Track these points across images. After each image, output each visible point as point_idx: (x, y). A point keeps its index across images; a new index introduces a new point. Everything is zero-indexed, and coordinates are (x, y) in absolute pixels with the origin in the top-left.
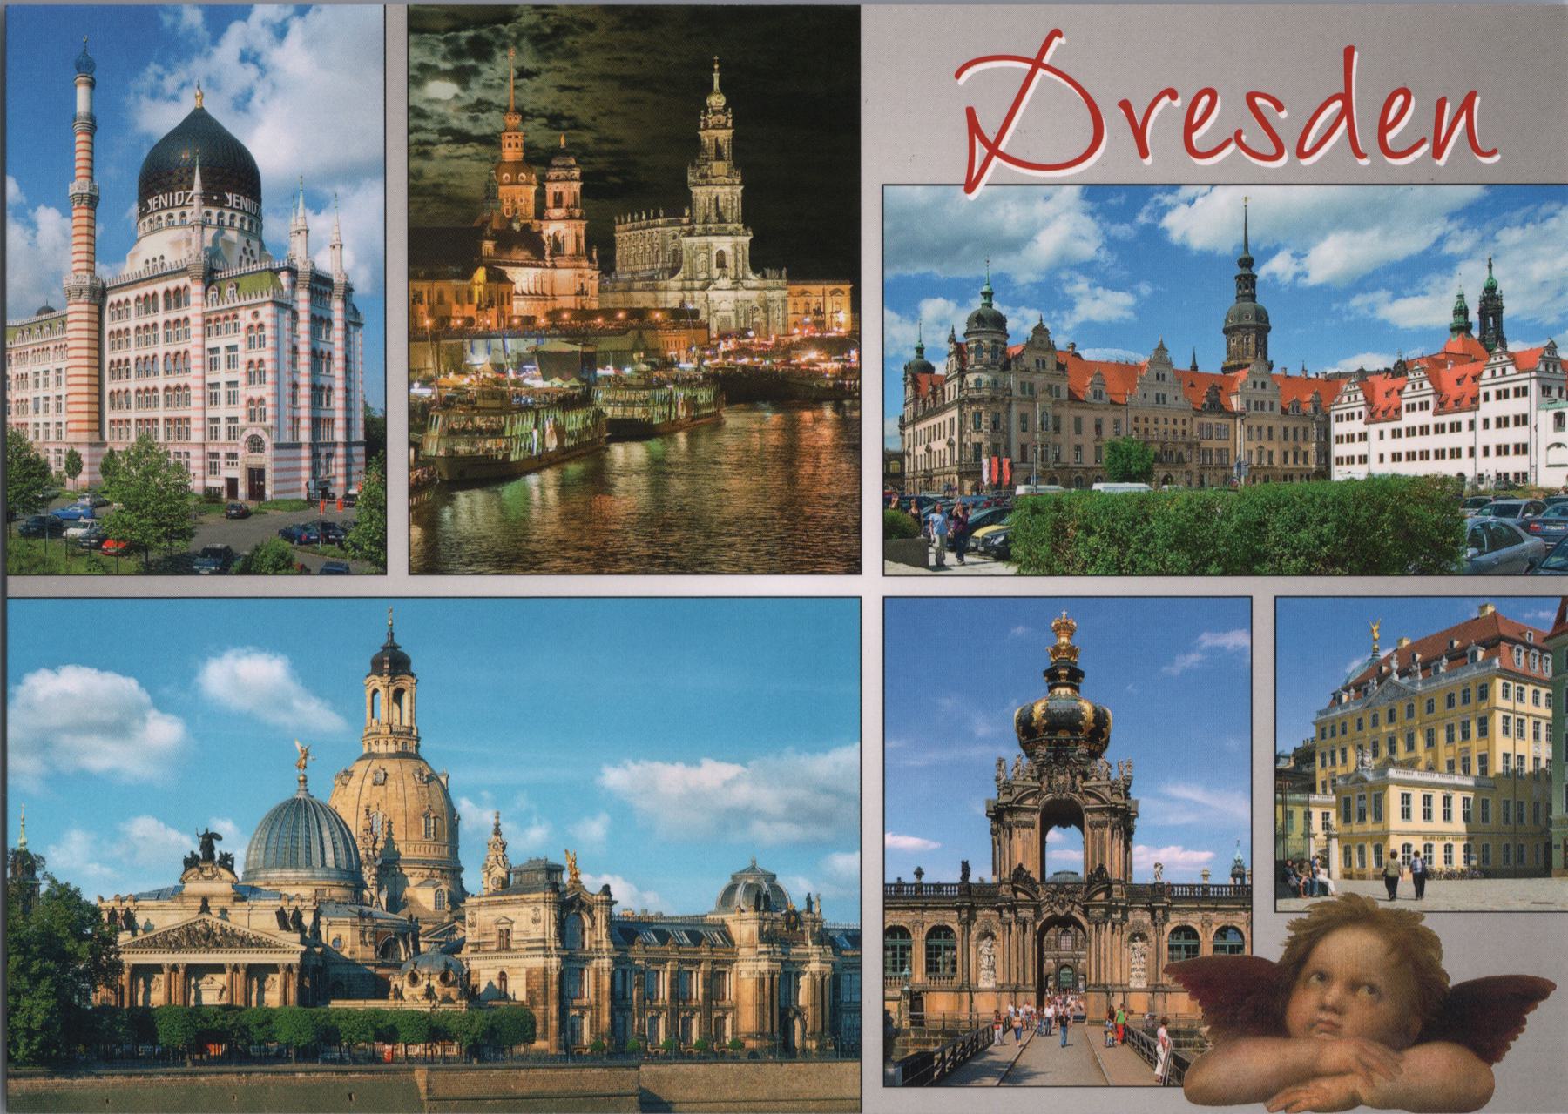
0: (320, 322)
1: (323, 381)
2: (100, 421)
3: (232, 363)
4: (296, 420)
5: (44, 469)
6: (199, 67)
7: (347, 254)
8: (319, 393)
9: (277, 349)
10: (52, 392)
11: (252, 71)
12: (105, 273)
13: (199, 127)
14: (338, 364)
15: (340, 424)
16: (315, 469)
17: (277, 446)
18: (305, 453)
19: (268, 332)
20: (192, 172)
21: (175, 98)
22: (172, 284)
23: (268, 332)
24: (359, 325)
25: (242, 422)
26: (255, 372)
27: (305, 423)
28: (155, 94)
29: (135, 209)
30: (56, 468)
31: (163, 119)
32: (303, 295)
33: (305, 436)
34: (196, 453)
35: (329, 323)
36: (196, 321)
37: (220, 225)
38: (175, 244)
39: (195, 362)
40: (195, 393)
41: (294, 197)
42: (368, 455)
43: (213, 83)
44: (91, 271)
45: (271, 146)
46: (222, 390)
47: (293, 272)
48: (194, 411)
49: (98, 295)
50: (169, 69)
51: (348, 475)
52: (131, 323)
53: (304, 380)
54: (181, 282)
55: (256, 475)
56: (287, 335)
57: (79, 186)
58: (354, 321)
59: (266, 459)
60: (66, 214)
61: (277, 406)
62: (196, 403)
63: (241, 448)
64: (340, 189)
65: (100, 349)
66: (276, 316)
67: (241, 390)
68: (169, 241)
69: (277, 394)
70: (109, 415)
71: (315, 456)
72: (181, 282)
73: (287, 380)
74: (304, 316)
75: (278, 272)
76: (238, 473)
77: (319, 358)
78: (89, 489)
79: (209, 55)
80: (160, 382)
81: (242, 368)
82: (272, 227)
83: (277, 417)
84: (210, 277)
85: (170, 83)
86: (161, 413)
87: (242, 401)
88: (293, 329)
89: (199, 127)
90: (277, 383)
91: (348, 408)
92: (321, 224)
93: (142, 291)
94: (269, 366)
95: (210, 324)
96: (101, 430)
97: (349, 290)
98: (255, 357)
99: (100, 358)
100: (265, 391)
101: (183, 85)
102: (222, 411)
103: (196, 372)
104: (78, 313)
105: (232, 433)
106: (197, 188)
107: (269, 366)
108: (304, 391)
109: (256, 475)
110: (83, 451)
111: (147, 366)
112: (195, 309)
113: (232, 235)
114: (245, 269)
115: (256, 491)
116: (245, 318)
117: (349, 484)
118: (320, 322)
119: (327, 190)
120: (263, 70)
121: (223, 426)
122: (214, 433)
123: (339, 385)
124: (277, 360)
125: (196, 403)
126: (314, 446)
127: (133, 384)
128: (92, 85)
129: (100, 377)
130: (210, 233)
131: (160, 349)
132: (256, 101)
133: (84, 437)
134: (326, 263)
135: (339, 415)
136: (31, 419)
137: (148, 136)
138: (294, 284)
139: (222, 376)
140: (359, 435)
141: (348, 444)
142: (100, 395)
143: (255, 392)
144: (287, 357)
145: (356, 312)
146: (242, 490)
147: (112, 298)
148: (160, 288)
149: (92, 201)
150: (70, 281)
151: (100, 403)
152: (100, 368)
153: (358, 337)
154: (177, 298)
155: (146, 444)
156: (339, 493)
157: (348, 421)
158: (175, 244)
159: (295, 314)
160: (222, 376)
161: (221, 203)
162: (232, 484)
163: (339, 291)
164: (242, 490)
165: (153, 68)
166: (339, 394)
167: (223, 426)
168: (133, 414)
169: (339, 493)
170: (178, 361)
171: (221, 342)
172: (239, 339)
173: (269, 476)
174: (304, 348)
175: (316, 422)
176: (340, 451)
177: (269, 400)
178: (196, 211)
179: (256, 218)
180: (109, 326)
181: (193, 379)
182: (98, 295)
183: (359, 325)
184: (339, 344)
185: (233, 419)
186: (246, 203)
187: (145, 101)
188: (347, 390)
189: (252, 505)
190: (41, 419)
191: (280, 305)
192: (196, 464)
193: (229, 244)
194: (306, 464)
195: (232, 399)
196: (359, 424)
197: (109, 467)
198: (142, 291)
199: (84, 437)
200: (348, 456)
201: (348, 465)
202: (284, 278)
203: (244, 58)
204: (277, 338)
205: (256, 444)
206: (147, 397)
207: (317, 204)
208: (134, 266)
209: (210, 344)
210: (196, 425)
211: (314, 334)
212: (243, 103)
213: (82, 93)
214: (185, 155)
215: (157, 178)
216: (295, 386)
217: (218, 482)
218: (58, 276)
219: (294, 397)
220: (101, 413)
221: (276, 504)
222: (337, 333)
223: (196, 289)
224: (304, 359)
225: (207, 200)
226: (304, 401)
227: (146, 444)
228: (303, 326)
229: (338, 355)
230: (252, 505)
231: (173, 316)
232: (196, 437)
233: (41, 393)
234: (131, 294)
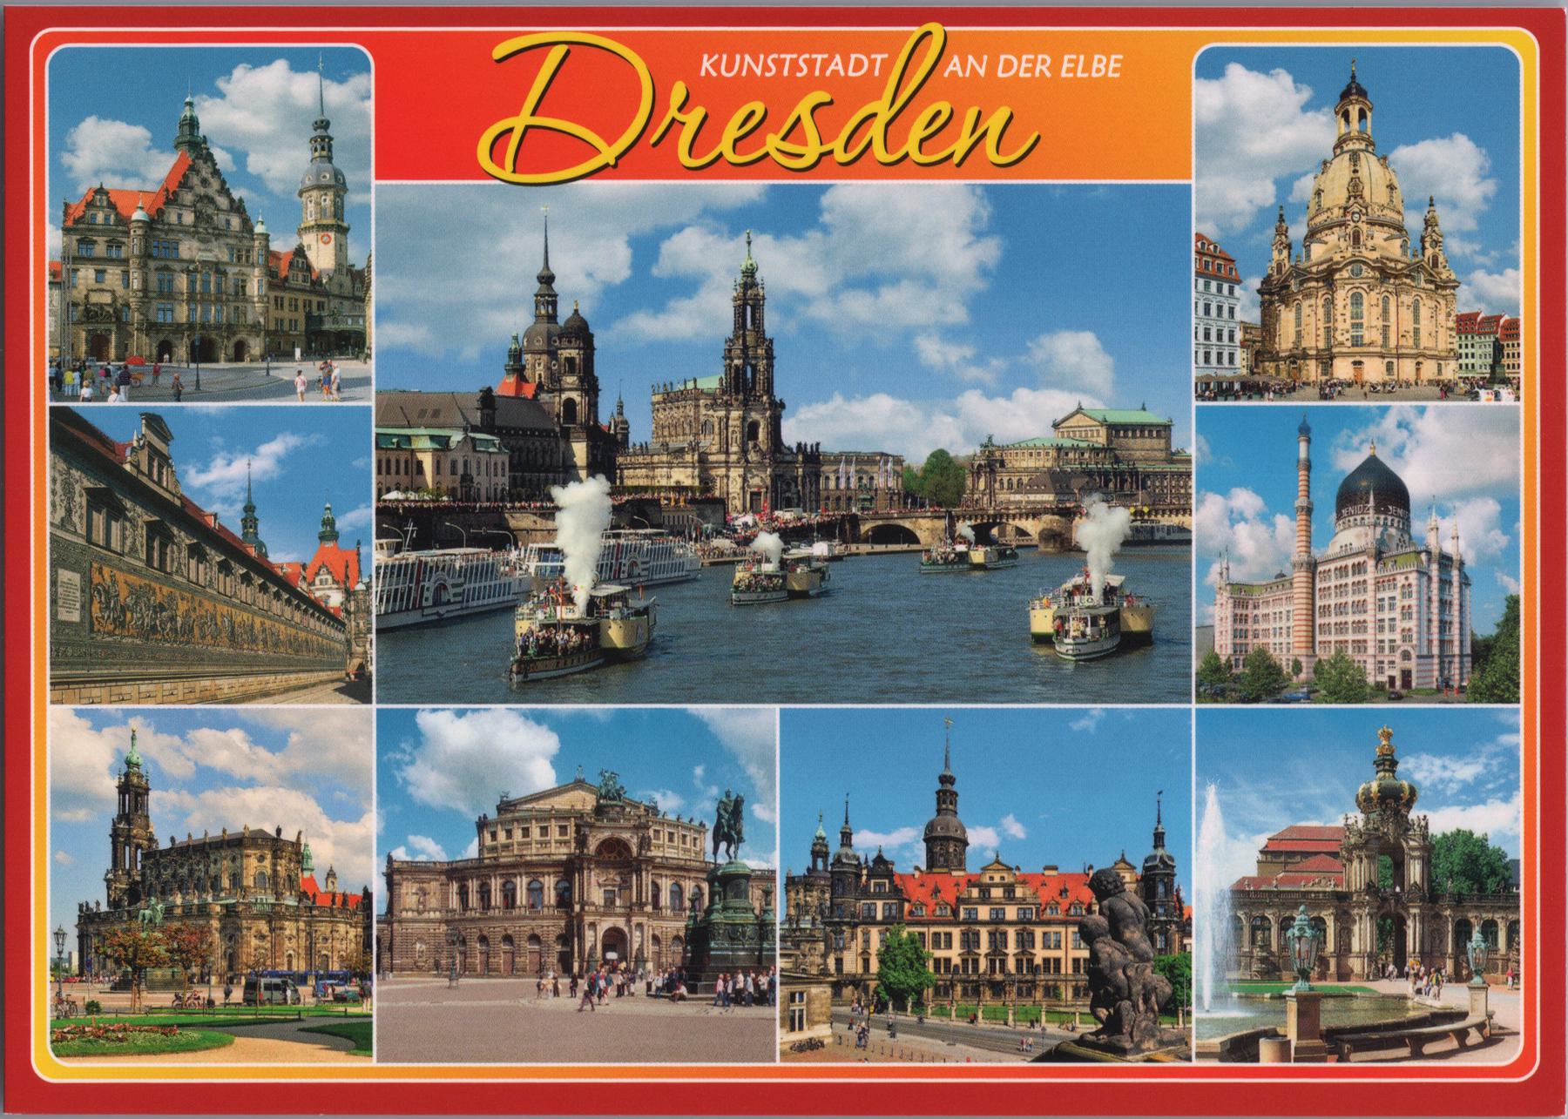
0: (1445, 583)
1: (1447, 618)
2: (1313, 642)
3: (1392, 607)
4: (1430, 642)
5: (1279, 671)
6: (1373, 431)
7: (1462, 542)
8: (1444, 625)
9: (1419, 599)
10: (1284, 624)
11: (1405, 433)
12: (1317, 554)
13: (1373, 467)
14: (1456, 607)
15: (1457, 643)
16: (1441, 670)
17: (1419, 657)
18: (1436, 660)
19: (1414, 589)
20: (1368, 493)
21: (1358, 450)
22: (1356, 560)
23: (1414, 589)
24: (1468, 585)
25: (1399, 642)
26: (1406, 613)
27: (1436, 643)
28: (1347, 447)
29: (1334, 515)
30: (1287, 669)
31: (1350, 462)
32: (1435, 567)
33: (1436, 651)
34: (1370, 661)
35: (1451, 583)
36: (1371, 582)
37: (1385, 525)
38: (1358, 536)
39: (1370, 606)
40: (1370, 625)
41: (1430, 508)
42: (1473, 663)
43: (1382, 441)
44: (1309, 552)
45: (1416, 478)
46: (1386, 624)
47: (1429, 553)
48: (1369, 636)
49: (1312, 567)
50: (1355, 432)
51: (1461, 674)
52: (1333, 583)
53: (1435, 617)
54: (1361, 559)
55: (1406, 674)
56: (1425, 590)
57: (1301, 501)
58: (1465, 582)
59: (1412, 665)
60: (1293, 519)
61: (1419, 633)
62: (1370, 630)
63: (1397, 657)
64: (1457, 504)
65: (1313, 599)
66: (1419, 579)
67: (1398, 623)
68: (1355, 536)
69: (1419, 626)
70: (1318, 638)
71: (1442, 663)
72: (1361, 559)
73: (1425, 617)
74: (1435, 579)
75: (1420, 553)
76: (1396, 673)
77: (1444, 604)
78: (1307, 682)
79: (1379, 424)
80: (1350, 618)
81: (1399, 610)
82: (1417, 527)
83: (1419, 639)
84: (1379, 556)
85: (1355, 441)
86: (1350, 637)
87: (1399, 630)
88: (1429, 587)
89: (1373, 467)
90: (1419, 619)
91: (1461, 634)
92: (1446, 525)
93: (1339, 564)
94: (1414, 609)
95: (1379, 585)
96: (1313, 647)
97: (1462, 563)
98: (1406, 603)
99: (1313, 604)
100: (1412, 624)
101: (1363, 442)
102: (1387, 636)
103: (1370, 612)
104: (1300, 578)
105: (1392, 649)
106: (1372, 503)
107: (1414, 609)
108: (1435, 624)
109: (1406, 674)
110: (1303, 660)
111: (1341, 610)
112: (1370, 575)
113: (1393, 531)
114: (1400, 551)
115: (1406, 683)
116: (1401, 580)
117: (1462, 680)
118: (1445, 583)
119: (1450, 505)
120: (1411, 433)
121: (1387, 645)
122: (1382, 649)
123: (1456, 620)
124: (1419, 606)
125: (1370, 630)
126: (1441, 656)
127: (1333, 620)
128: (1309, 441)
129: (1313, 615)
130: (1379, 530)
131: (1350, 599)
132: (1407, 451)
133: (1304, 651)
134: (1449, 548)
135: (1456, 638)
136: (1271, 640)
137: (1343, 472)
138: (1429, 560)
139: (1386, 615)
140: (1468, 651)
141: (1461, 656)
142: (1313, 626)
143: (1407, 624)
144: (1425, 603)
145: (1466, 578)
146: (1398, 683)
147: (1320, 569)
148: (1350, 562)
149: (1309, 511)
150: (1295, 558)
151: (1313, 631)
152: (1313, 610)
153: (1467, 592)
154: (1359, 568)
155: (1340, 656)
156: (1456, 685)
157: (1461, 642)
158: (1358, 536)
159: (1430, 579)
160: (1386, 615)
161: (1386, 512)
162: (1392, 679)
163: (1456, 564)
164: (1398, 683)
165: (1345, 432)
166: (1456, 626)
167: (1387, 645)
168: (1333, 638)
169: (1456, 685)
170: (1360, 607)
171: (1386, 595)
172: (1397, 593)
173: (1414, 675)
174: (1435, 598)
175: (1442, 642)
176: (1457, 660)
177: (1415, 629)
178: (1371, 517)
179: (1406, 521)
180: (1318, 585)
181: (1369, 617)
182: (1312, 567)
183: (1468, 585)
184: (1456, 596)
185: (1392, 641)
186: (1400, 512)
187: (1341, 452)
188: (1461, 623)
189: (1404, 692)
190: (1277, 640)
191: (1420, 573)
192: (1370, 667)
193: (1390, 536)
194: (1436, 667)
195: (1392, 629)
196: (1468, 644)
197: (1318, 669)
198: (1339, 564)
199: (1304, 651)
200: (1461, 662)
201: (1461, 668)
202: (1424, 557)
203: (1400, 425)
204: (1419, 592)
205: (1406, 656)
206: (1341, 628)
207: (1444, 513)
208: (1333, 549)
209: (1380, 596)
210: (1370, 644)
211: (1441, 590)
212: (1399, 452)
213: (1303, 446)
214: (1364, 484)
215: (1348, 497)
216: (1430, 621)
217: (1383, 678)
218: (1288, 556)
219: (1429, 628)
220: (1313, 637)
221: (1418, 691)
222: (1455, 589)
223: (1371, 563)
224: (1435, 605)
225: (1377, 511)
226: (1435, 630)
227: (1340, 656)
228: (1435, 585)
229: (1456, 602)
230: (1404, 692)
231: (1357, 578)
232: (1371, 651)
233: (1278, 625)
234: (1332, 566)
